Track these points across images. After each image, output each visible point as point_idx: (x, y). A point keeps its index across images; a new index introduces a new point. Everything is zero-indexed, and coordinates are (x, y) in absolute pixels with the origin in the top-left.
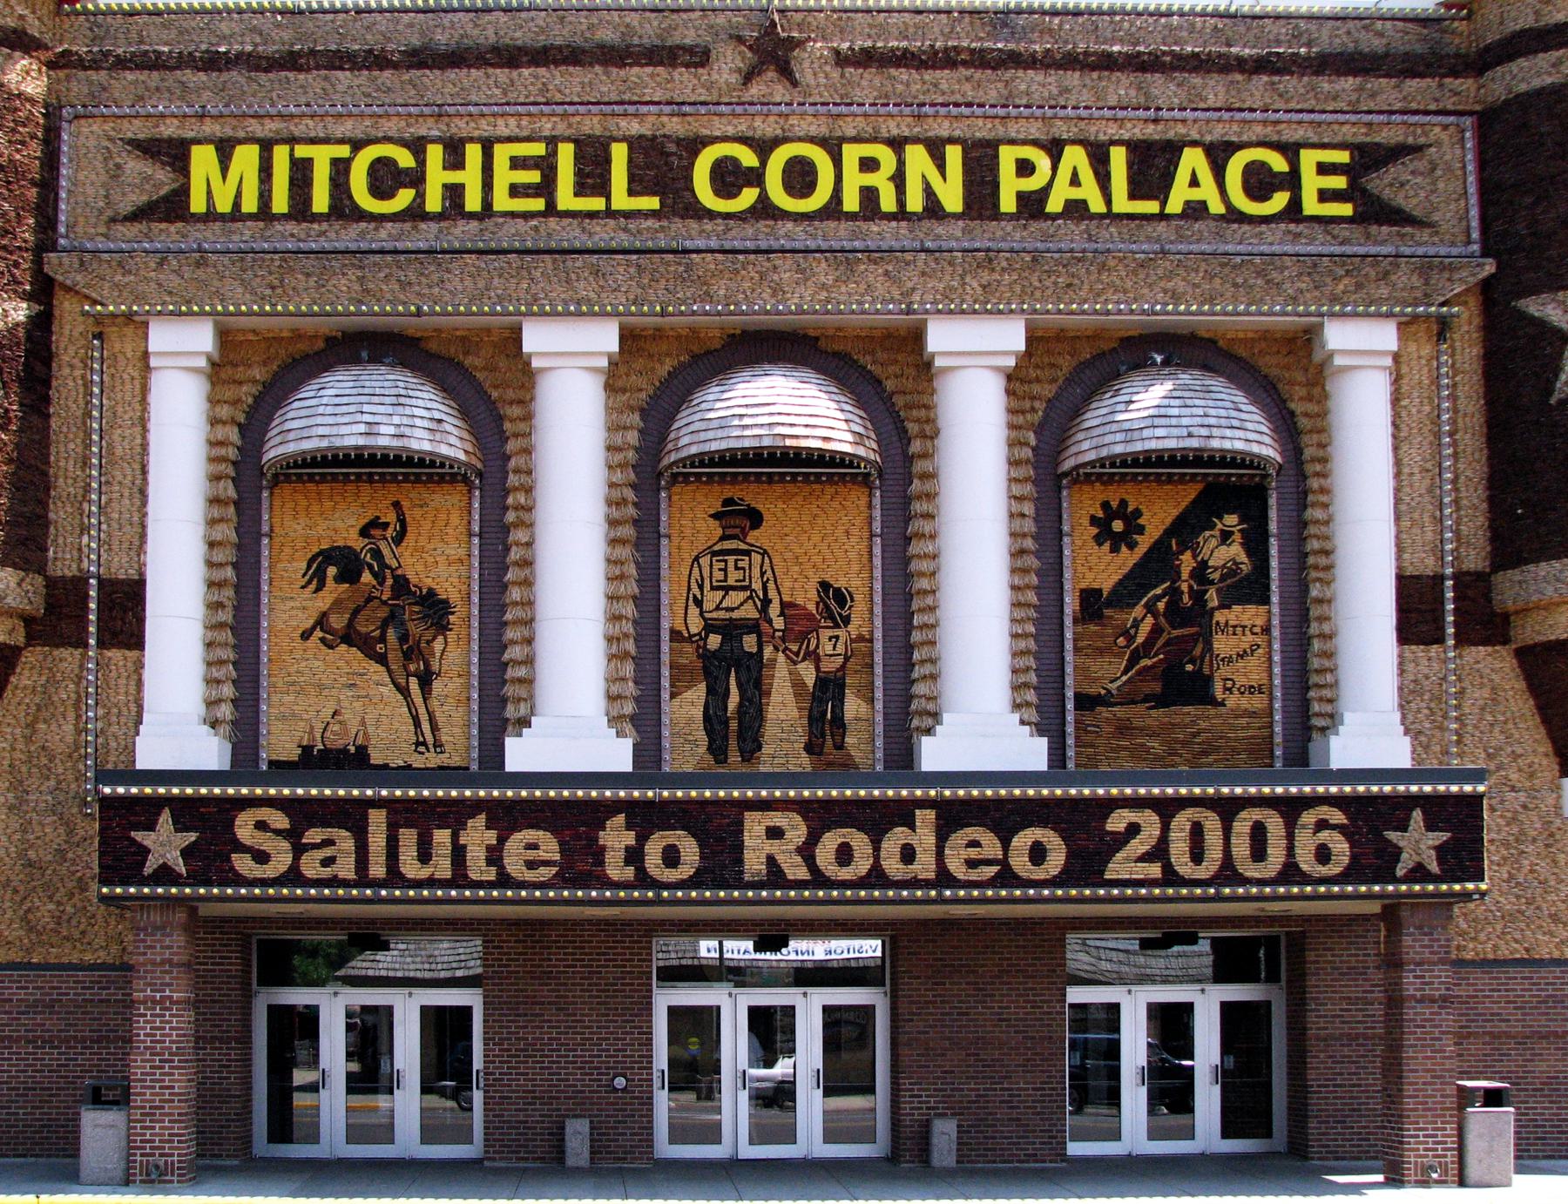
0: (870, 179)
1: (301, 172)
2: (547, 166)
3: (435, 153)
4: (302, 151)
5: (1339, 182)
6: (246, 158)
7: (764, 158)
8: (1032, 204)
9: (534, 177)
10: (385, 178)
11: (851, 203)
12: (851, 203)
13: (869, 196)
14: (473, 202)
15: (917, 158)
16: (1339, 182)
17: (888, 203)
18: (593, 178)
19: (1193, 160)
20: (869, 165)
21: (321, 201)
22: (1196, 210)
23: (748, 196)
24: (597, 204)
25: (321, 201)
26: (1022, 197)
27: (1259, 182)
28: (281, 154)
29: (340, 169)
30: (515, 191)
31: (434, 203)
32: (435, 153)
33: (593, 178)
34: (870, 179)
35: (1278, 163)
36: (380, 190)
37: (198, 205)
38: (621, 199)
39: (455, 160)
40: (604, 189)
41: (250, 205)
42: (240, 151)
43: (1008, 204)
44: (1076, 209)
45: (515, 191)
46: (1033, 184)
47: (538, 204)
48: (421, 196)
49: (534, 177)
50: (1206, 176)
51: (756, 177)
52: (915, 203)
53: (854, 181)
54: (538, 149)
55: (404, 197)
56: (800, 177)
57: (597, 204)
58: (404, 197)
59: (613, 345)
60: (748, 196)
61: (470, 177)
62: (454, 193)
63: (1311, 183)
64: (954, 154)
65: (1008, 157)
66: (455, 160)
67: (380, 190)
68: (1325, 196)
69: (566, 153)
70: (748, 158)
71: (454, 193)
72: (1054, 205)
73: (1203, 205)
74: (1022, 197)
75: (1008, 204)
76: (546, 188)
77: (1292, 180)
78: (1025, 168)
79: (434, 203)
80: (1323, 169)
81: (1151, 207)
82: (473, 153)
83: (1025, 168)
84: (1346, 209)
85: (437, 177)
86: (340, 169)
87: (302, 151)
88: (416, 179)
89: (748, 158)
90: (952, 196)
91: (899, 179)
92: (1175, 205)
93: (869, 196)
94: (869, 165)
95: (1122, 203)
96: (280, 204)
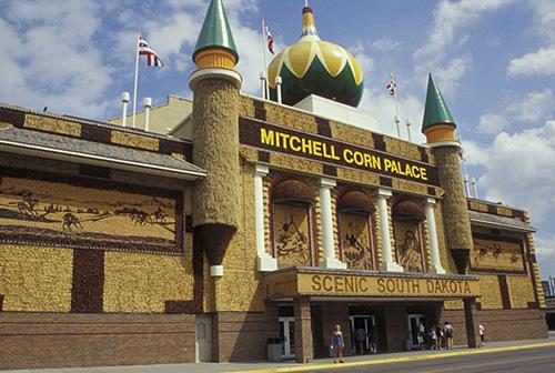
1: (281, 138)
2: (321, 147)
18: (329, 152)
23: (351, 161)
29: (288, 140)
33: (329, 152)
41: (272, 144)
51: (352, 157)
53: (366, 161)
55: (299, 148)
58: (299, 148)
60: (351, 161)
61: (309, 146)
62: (307, 149)
65: (386, 161)
76: (322, 152)
85: (304, 145)
86: (288, 140)
96: (278, 145)
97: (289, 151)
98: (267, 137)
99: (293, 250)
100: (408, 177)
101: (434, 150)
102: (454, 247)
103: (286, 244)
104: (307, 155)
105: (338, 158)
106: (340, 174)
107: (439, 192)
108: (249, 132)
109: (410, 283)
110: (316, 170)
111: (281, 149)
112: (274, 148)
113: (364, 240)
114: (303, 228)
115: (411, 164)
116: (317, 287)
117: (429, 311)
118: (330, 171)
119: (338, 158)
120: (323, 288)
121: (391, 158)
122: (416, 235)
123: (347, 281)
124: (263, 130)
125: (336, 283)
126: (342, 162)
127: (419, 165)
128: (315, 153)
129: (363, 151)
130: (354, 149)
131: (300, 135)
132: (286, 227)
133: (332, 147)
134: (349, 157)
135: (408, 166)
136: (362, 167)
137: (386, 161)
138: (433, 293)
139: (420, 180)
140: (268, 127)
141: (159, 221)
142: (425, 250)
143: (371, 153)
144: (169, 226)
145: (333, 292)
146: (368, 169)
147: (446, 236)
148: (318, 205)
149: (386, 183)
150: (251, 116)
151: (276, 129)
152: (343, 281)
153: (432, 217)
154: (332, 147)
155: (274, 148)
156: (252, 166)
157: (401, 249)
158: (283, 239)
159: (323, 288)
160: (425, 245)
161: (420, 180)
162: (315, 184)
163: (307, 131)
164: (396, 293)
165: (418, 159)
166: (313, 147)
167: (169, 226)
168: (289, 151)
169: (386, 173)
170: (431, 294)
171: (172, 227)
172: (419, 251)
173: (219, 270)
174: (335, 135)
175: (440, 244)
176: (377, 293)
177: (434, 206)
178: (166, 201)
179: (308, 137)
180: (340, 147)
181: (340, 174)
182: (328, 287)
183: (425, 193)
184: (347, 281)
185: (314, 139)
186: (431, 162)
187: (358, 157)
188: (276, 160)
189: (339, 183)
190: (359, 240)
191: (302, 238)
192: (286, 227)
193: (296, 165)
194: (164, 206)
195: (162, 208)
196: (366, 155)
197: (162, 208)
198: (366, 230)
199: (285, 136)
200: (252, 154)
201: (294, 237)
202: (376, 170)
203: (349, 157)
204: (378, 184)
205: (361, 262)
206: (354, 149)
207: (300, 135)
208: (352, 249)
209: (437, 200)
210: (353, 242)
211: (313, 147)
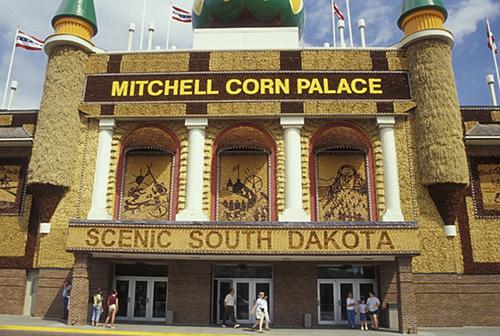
0: (267, 87)
2: (193, 85)
3: (167, 82)
4: (138, 82)
5: (379, 86)
6: (125, 83)
7: (242, 82)
8: (305, 91)
9: (190, 87)
10: (156, 88)
11: (263, 92)
12: (263, 92)
13: (267, 90)
14: (175, 93)
15: (278, 81)
16: (379, 86)
17: (271, 92)
18: (203, 87)
19: (343, 81)
20: (267, 84)
21: (141, 93)
22: (344, 92)
23: (239, 90)
24: (204, 93)
25: (141, 93)
26: (303, 90)
27: (359, 86)
28: (133, 83)
29: (146, 86)
30: (186, 90)
31: (166, 93)
32: (167, 82)
33: (203, 87)
34: (267, 87)
35: (364, 82)
36: (155, 90)
37: (113, 94)
38: (209, 92)
39: (172, 84)
40: (206, 90)
41: (125, 94)
42: (124, 82)
43: (300, 92)
44: (316, 92)
45: (186, 90)
46: (306, 87)
47: (191, 93)
48: (163, 93)
49: (190, 87)
50: (347, 85)
51: (241, 87)
52: (278, 92)
54: (191, 81)
55: (160, 92)
56: (251, 86)
57: (204, 93)
58: (160, 92)
59: (206, 124)
60: (239, 90)
62: (171, 91)
63: (372, 86)
64: (287, 81)
65: (300, 81)
66: (172, 84)
67: (155, 90)
68: (375, 89)
69: (197, 81)
70: (239, 83)
71: (171, 91)
72: (311, 92)
73: (346, 92)
74: (303, 90)
75: (300, 92)
76: (193, 89)
77: (367, 86)
78: (304, 84)
79: (166, 93)
80: (375, 83)
81: (334, 92)
82: (176, 82)
83: (304, 84)
84: (381, 92)
85: (168, 87)
86: (146, 86)
87: (138, 82)
88: (163, 88)
89: (239, 83)
90: (287, 91)
91: (274, 87)
92: (339, 92)
93: (267, 90)
94: (267, 84)
95: (327, 91)
96: (132, 94)
97: (147, 97)
98: (117, 89)
99: (146, 204)
100: (344, 95)
101: (404, 51)
102: (425, 181)
103: (137, 197)
104: (171, 97)
105: (217, 92)
106: (213, 110)
107: (400, 106)
108: (97, 89)
109: (254, 237)
110: (177, 110)
111: (136, 98)
112: (128, 98)
113: (259, 183)
114: (164, 178)
115: (350, 77)
116: (93, 241)
117: (378, 274)
118: (197, 108)
119: (217, 92)
120: (100, 243)
121: (310, 77)
122: (361, 171)
123: (138, 235)
124: (115, 84)
125: (121, 237)
126: (224, 95)
127: (366, 77)
128: (182, 93)
129: (258, 77)
130: (242, 77)
131: (163, 78)
132: (139, 180)
133: (209, 82)
134: (234, 87)
135: (343, 81)
136: (258, 96)
137: (300, 81)
138: (303, 249)
139: (367, 95)
140: (120, 79)
141: (4, 186)
142: (375, 189)
143: (273, 76)
144: (12, 190)
145: (116, 247)
146: (267, 96)
147: (417, 163)
148: (185, 150)
149: (292, 106)
150: (103, 71)
151: (130, 78)
152: (133, 235)
153: (391, 147)
154: (209, 82)
155: (128, 98)
156: (96, 121)
157: (321, 189)
158: (134, 193)
159: (100, 243)
160: (374, 183)
161: (367, 95)
162: (183, 130)
163: (174, 71)
164: (223, 248)
165: (366, 65)
166: (181, 88)
167: (12, 190)
168: (147, 97)
169: (300, 96)
170: (292, 251)
171: (14, 191)
172: (366, 192)
173: (44, 228)
174: (214, 66)
175: (402, 178)
176: (187, 248)
177: (396, 127)
178: (12, 168)
179: (172, 78)
180: (220, 80)
181: (213, 110)
182: (108, 242)
183: (370, 107)
184: (138, 235)
185: (181, 77)
186: (394, 65)
187: (251, 86)
188: (121, 110)
189: (213, 122)
190: (249, 186)
191: (160, 189)
192: (139, 180)
193: (149, 110)
194: (10, 172)
195: (8, 175)
196: (263, 81)
197: (8, 175)
198: (262, 173)
199: (142, 83)
200: (95, 109)
201: (149, 190)
202: (282, 95)
203: (234, 87)
204: (278, 113)
205: (250, 213)
206: (242, 77)
207: (163, 78)
208: (235, 197)
209: (398, 118)
210: (238, 187)
211: (181, 88)
